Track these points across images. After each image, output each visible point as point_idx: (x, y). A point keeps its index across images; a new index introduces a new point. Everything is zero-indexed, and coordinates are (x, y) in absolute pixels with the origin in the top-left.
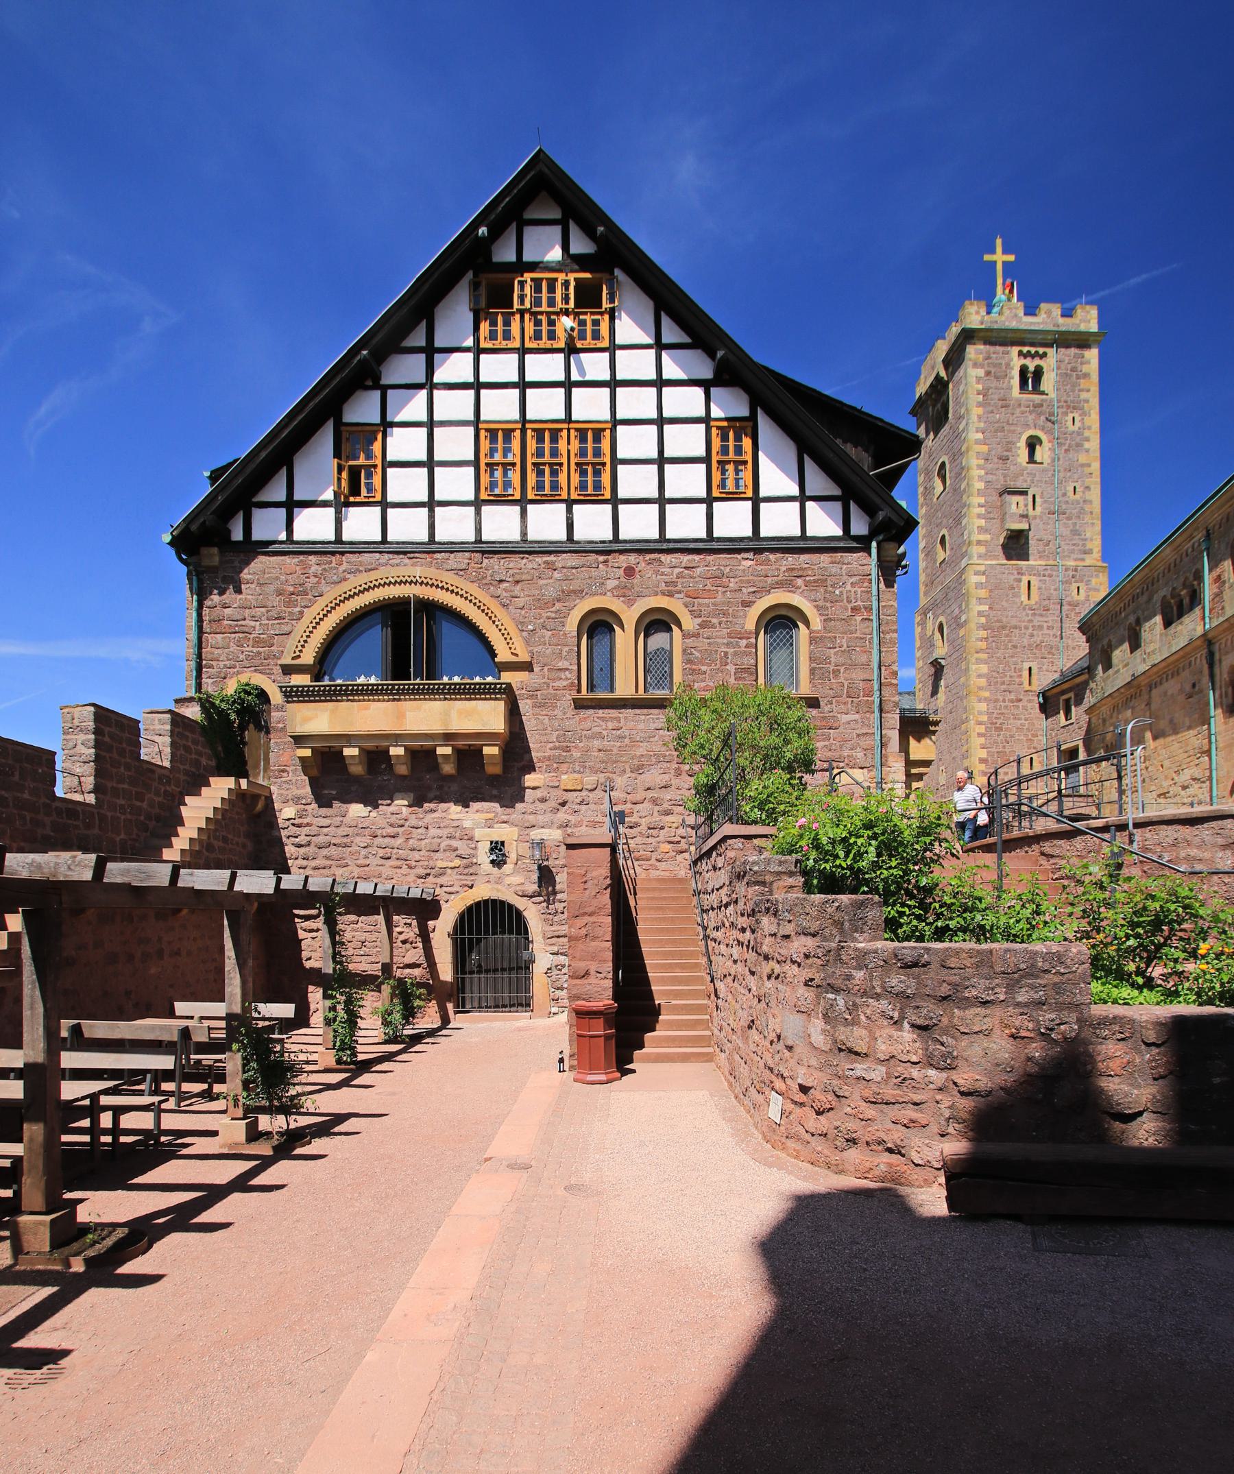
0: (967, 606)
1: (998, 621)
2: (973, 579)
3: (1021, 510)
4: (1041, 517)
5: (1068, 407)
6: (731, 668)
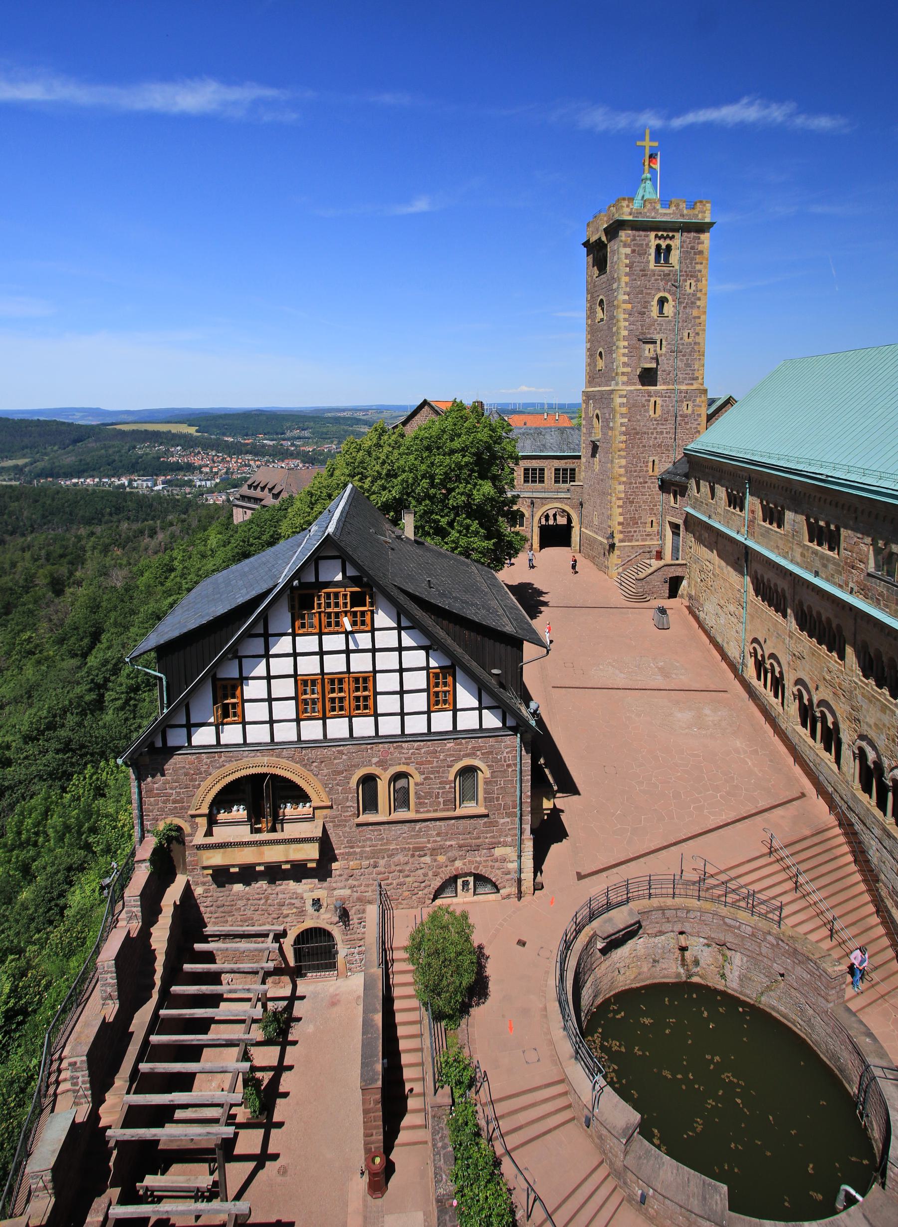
0: (614, 416)
1: (634, 429)
2: (619, 401)
3: (652, 354)
4: (665, 355)
5: (687, 275)
6: (441, 800)
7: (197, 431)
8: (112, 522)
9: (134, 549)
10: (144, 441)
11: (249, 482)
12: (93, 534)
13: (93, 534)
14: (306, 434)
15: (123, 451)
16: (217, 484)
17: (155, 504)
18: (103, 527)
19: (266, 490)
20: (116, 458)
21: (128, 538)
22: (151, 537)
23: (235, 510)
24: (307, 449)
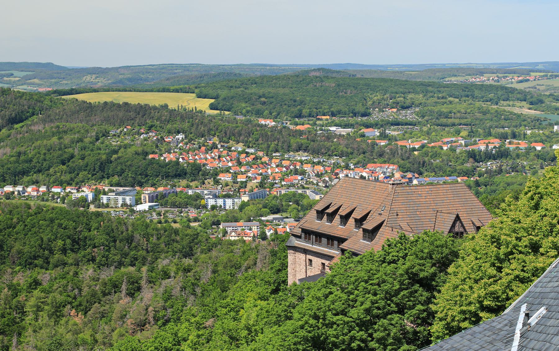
7: (213, 107)
8: (65, 264)
9: (103, 315)
10: (122, 123)
11: (320, 207)
12: (36, 283)
13: (36, 283)
14: (409, 115)
15: (87, 140)
16: (243, 206)
17: (137, 236)
18: (54, 273)
19: (351, 221)
20: (76, 152)
21: (94, 295)
22: (131, 295)
23: (291, 256)
24: (410, 144)
